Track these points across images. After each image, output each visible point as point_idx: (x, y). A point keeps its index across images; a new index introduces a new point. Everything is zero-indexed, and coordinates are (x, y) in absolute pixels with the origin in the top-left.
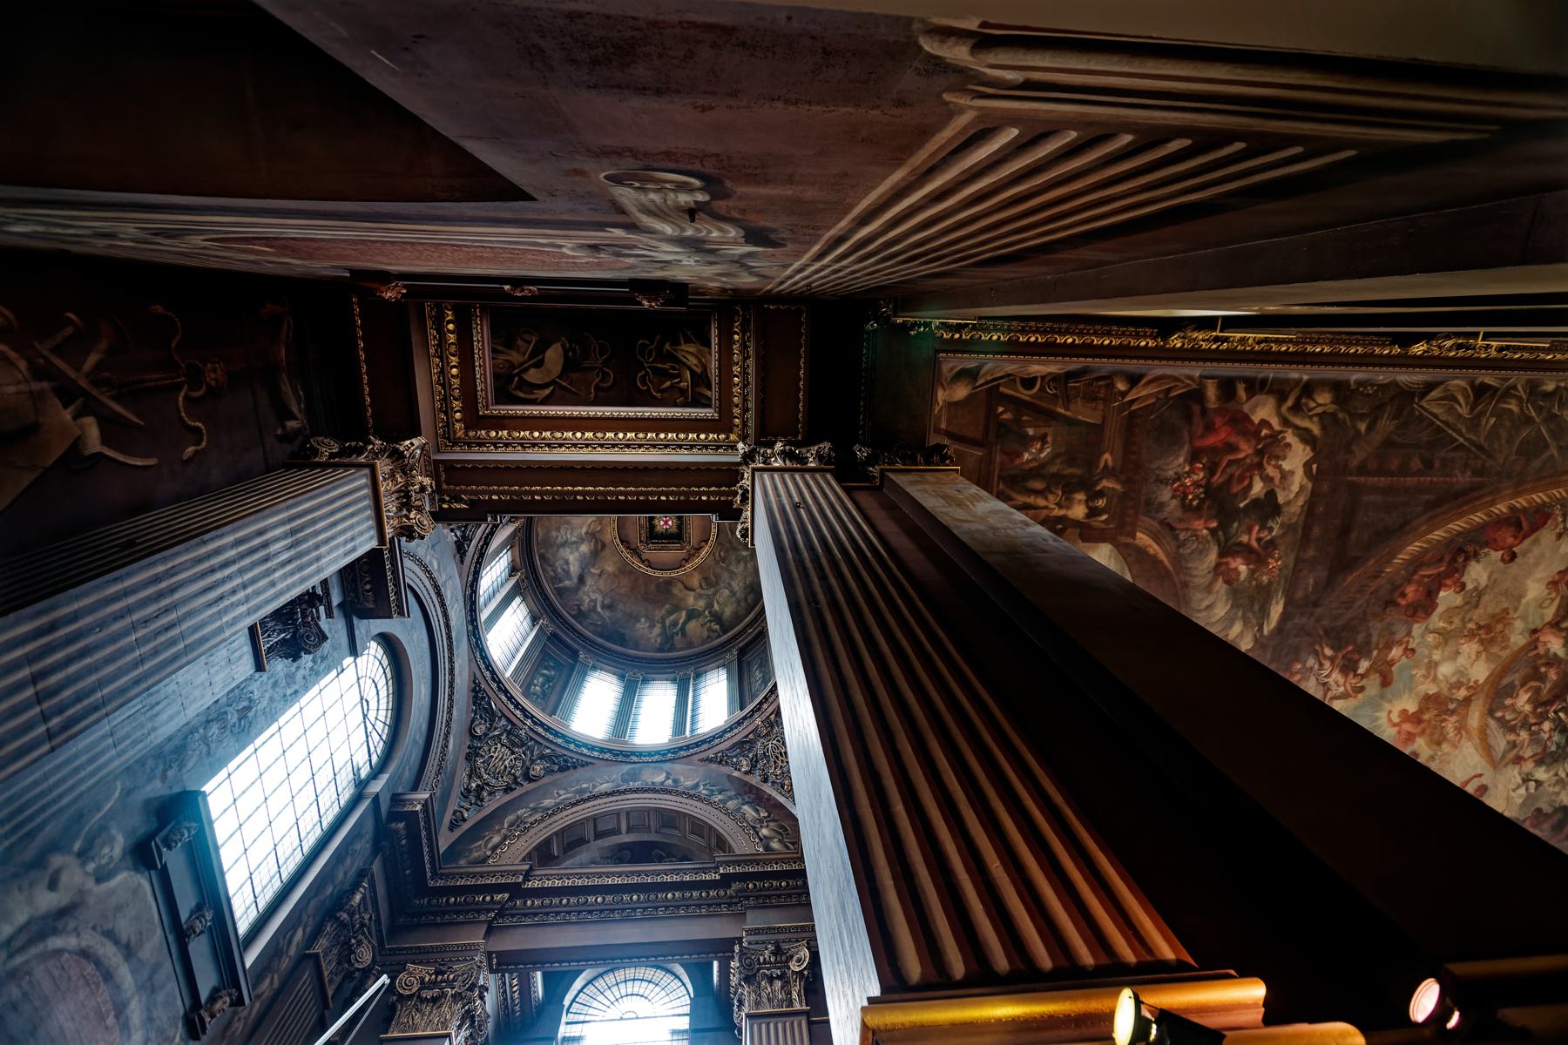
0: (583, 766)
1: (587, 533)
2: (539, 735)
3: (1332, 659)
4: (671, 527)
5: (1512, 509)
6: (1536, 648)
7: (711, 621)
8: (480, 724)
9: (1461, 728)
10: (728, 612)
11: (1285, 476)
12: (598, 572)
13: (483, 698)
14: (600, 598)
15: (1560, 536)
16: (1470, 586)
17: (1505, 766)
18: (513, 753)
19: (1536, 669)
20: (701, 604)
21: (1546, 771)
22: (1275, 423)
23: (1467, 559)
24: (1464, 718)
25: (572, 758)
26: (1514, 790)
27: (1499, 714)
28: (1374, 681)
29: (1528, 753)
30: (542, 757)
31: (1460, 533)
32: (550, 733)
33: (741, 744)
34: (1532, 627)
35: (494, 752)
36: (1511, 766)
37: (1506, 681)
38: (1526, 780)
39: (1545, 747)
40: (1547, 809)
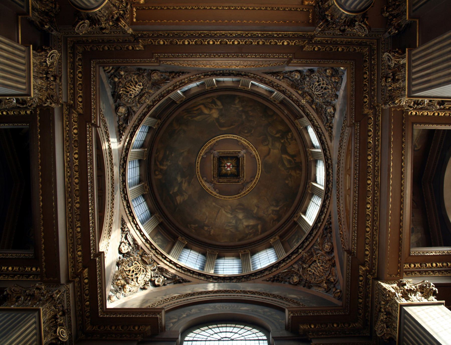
0: (330, 218)
1: (231, 214)
2: (308, 245)
4: (231, 163)
7: (287, 139)
8: (292, 279)
10: (280, 127)
12: (256, 208)
13: (278, 277)
14: (272, 208)
18: (315, 261)
20: (278, 145)
25: (325, 225)
30: (323, 244)
32: (309, 238)
33: (317, 111)
35: (312, 272)
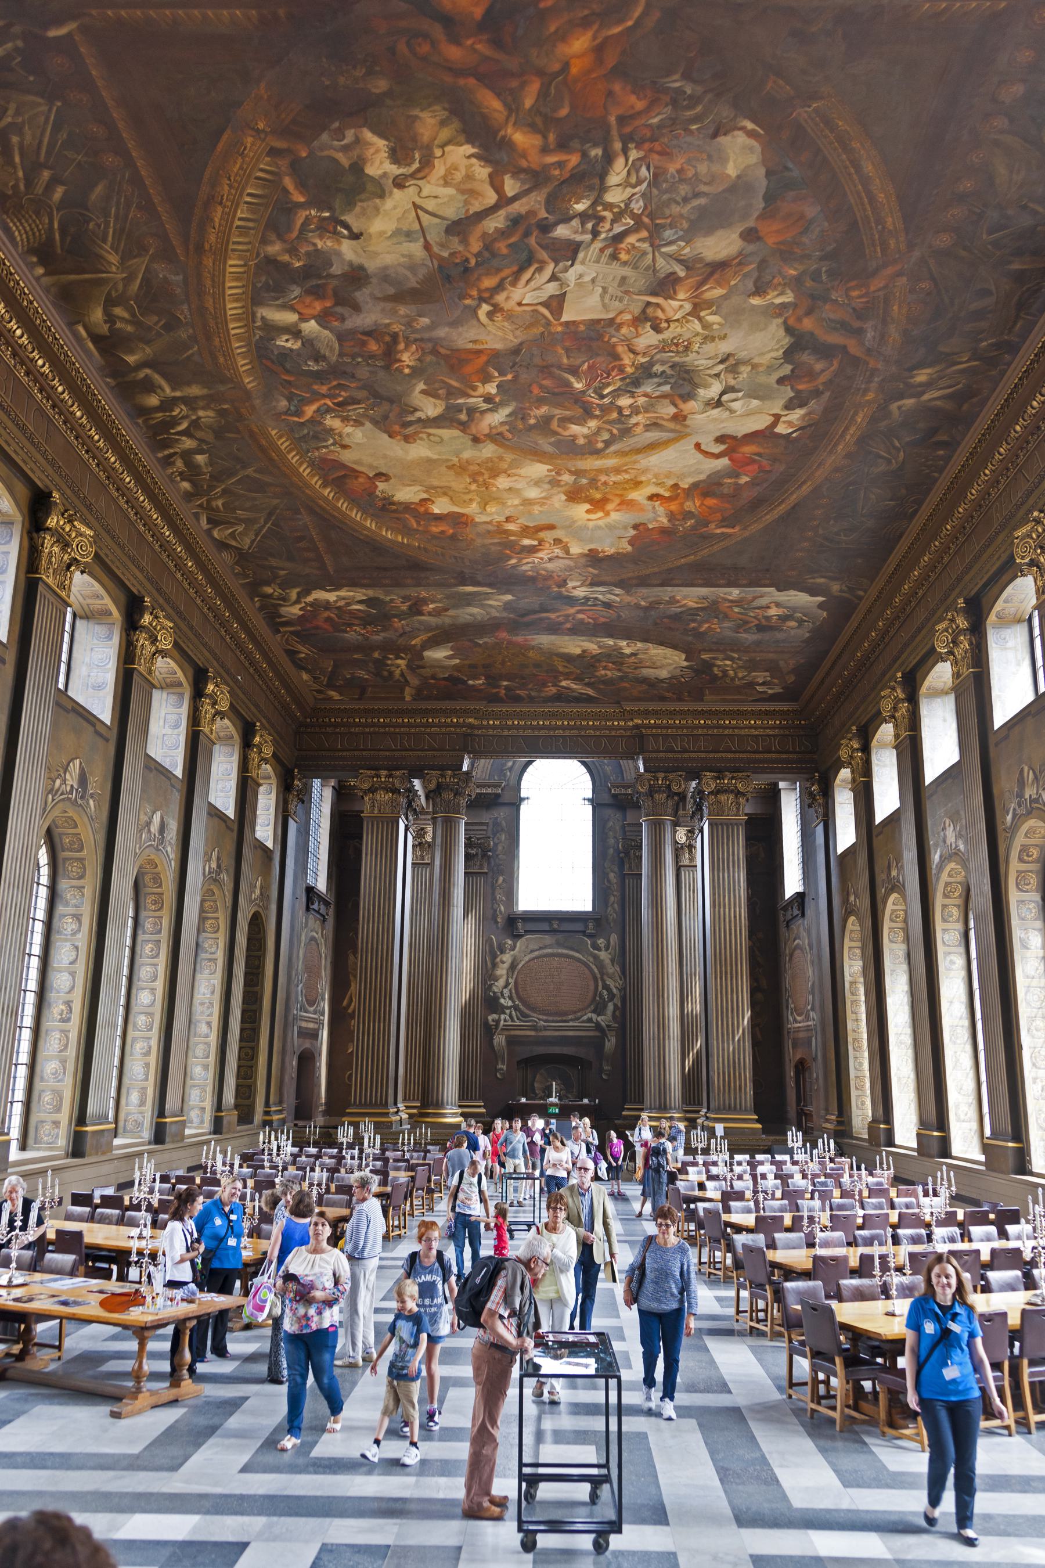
3: (520, 560)
5: (325, 485)
6: (500, 434)
9: (617, 470)
11: (340, 598)
15: (345, 447)
16: (425, 496)
17: (687, 426)
19: (531, 428)
21: (707, 386)
22: (299, 606)
23: (393, 504)
24: (600, 471)
26: (732, 411)
27: (600, 445)
28: (548, 536)
29: (672, 410)
31: (365, 512)
34: (470, 443)
36: (688, 422)
37: (549, 449)
38: (719, 404)
39: (664, 396)
40: (787, 369)
